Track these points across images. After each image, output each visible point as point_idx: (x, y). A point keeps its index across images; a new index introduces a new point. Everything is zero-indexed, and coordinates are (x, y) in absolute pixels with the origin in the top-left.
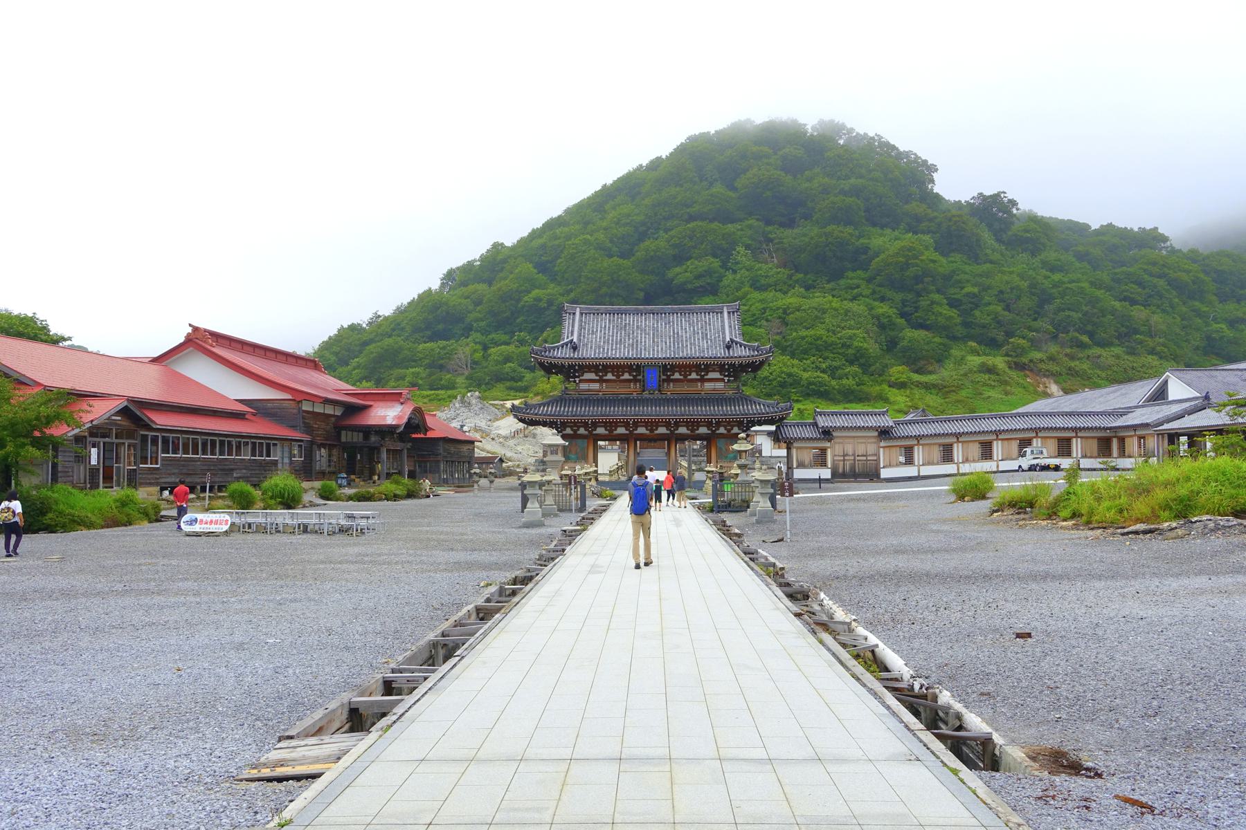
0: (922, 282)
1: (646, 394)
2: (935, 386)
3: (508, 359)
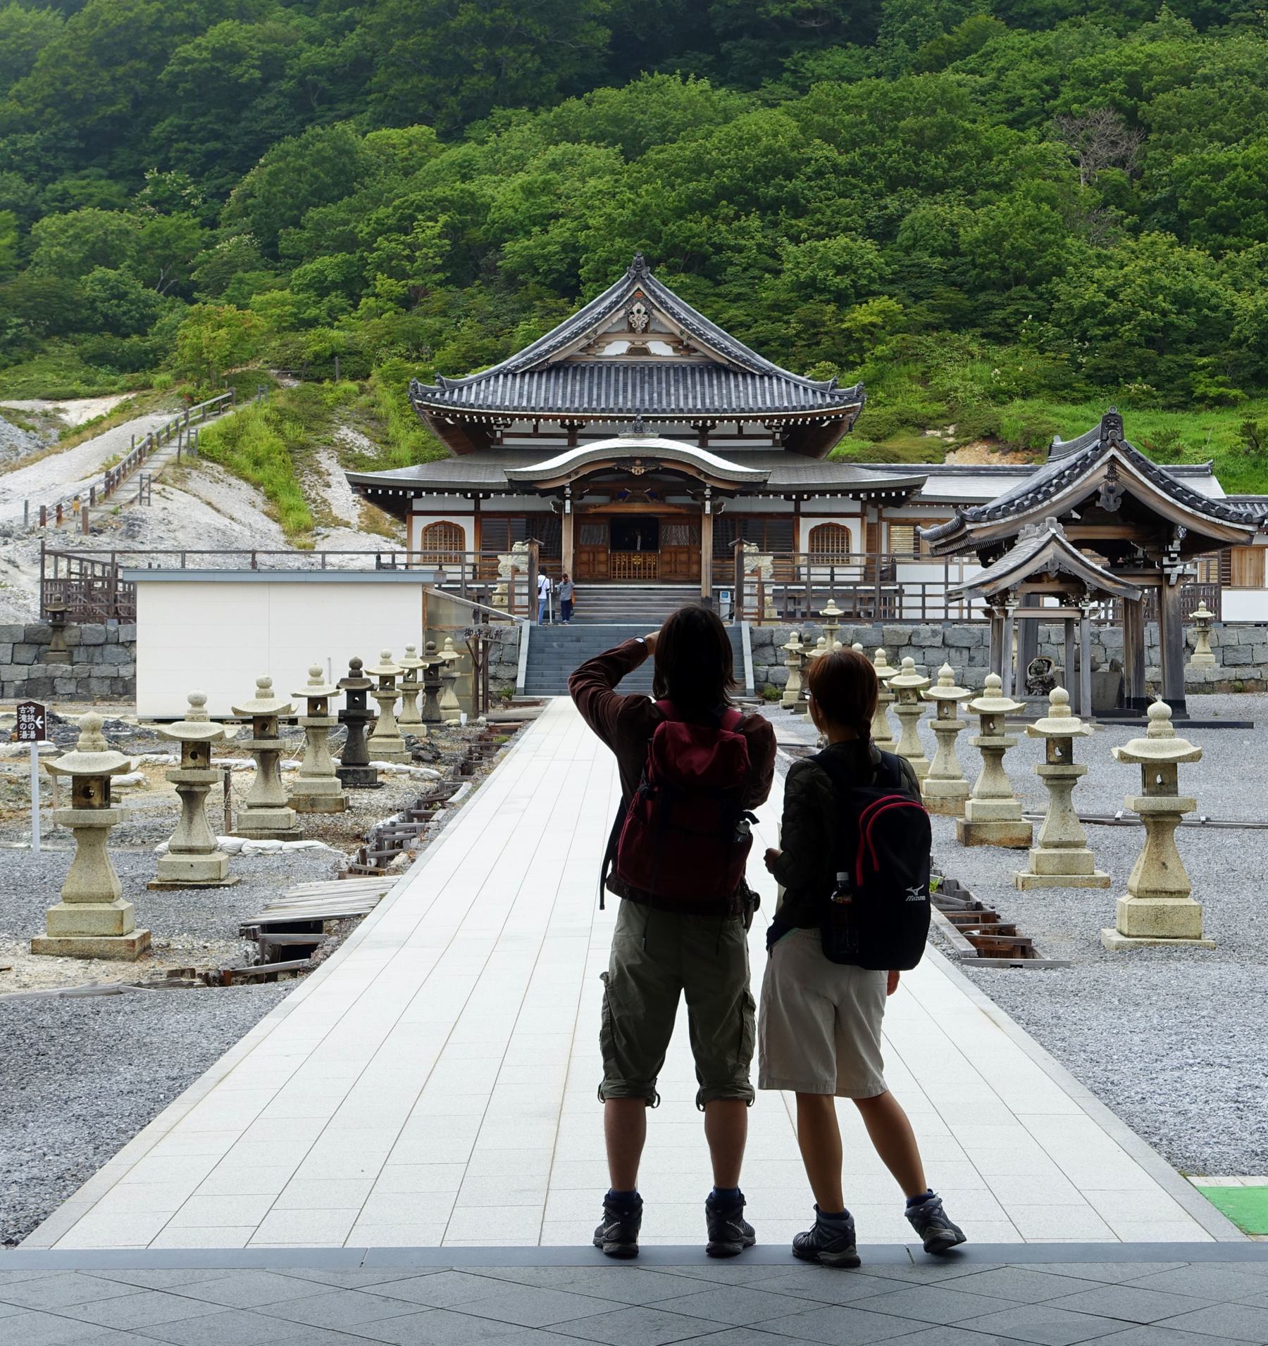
3: (103, 254)
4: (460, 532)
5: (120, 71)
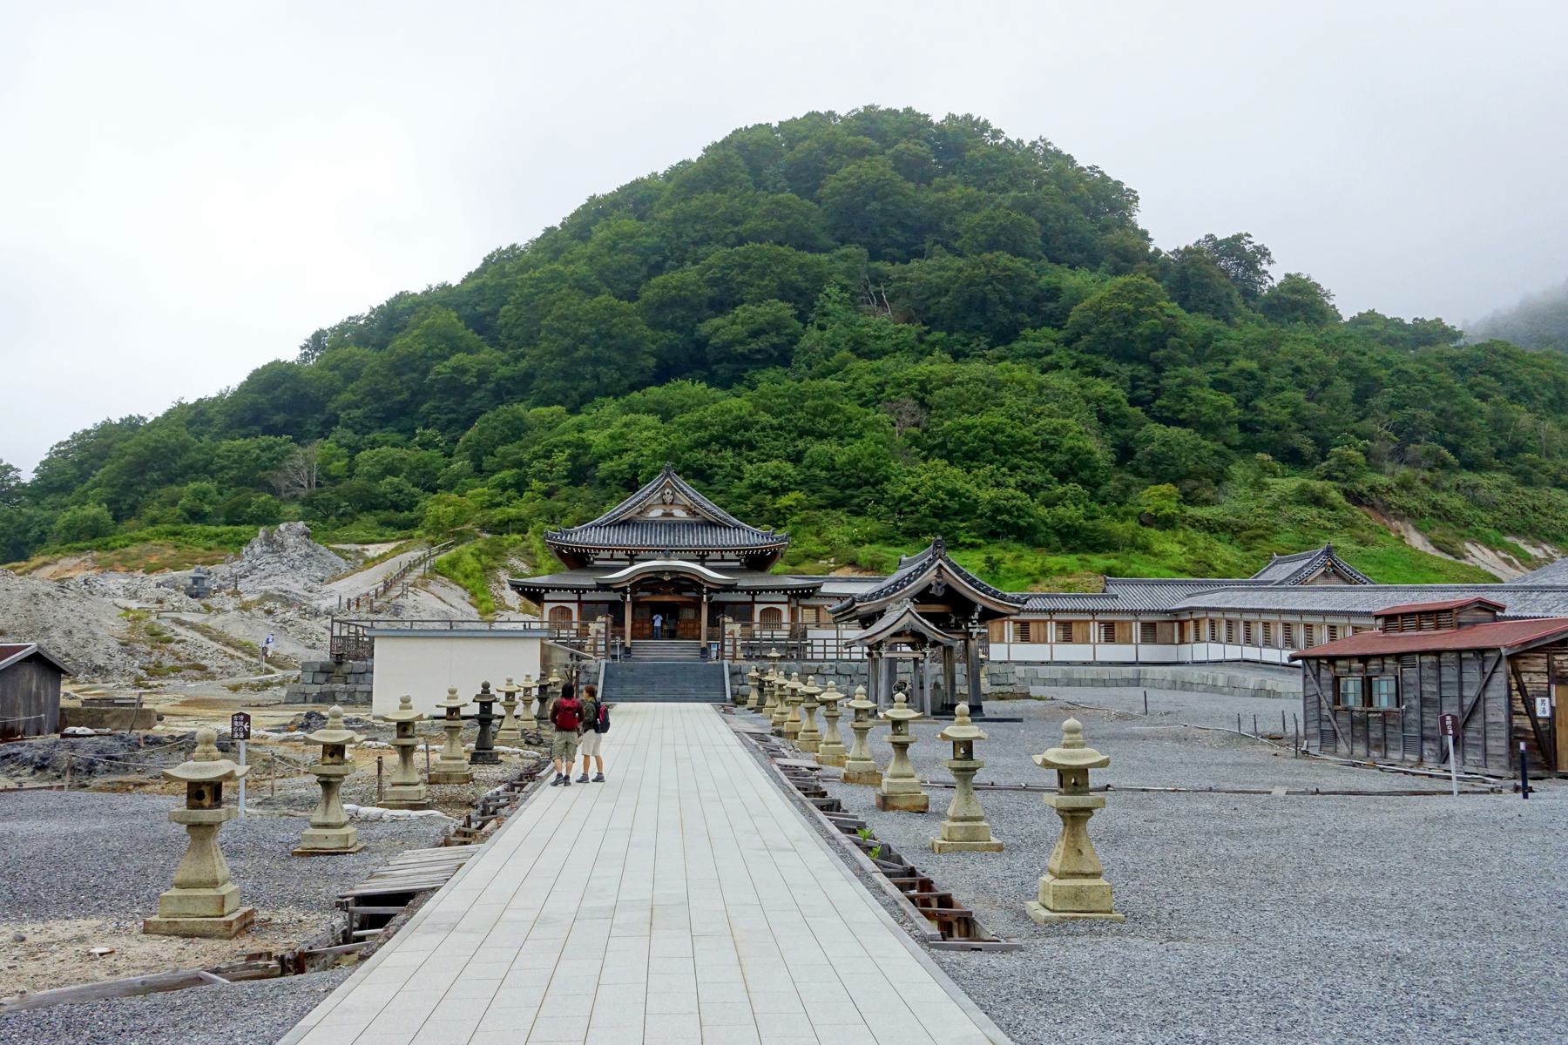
0: (1165, 347)
2: (1224, 527)
3: (392, 470)
4: (570, 611)
5: (404, 378)
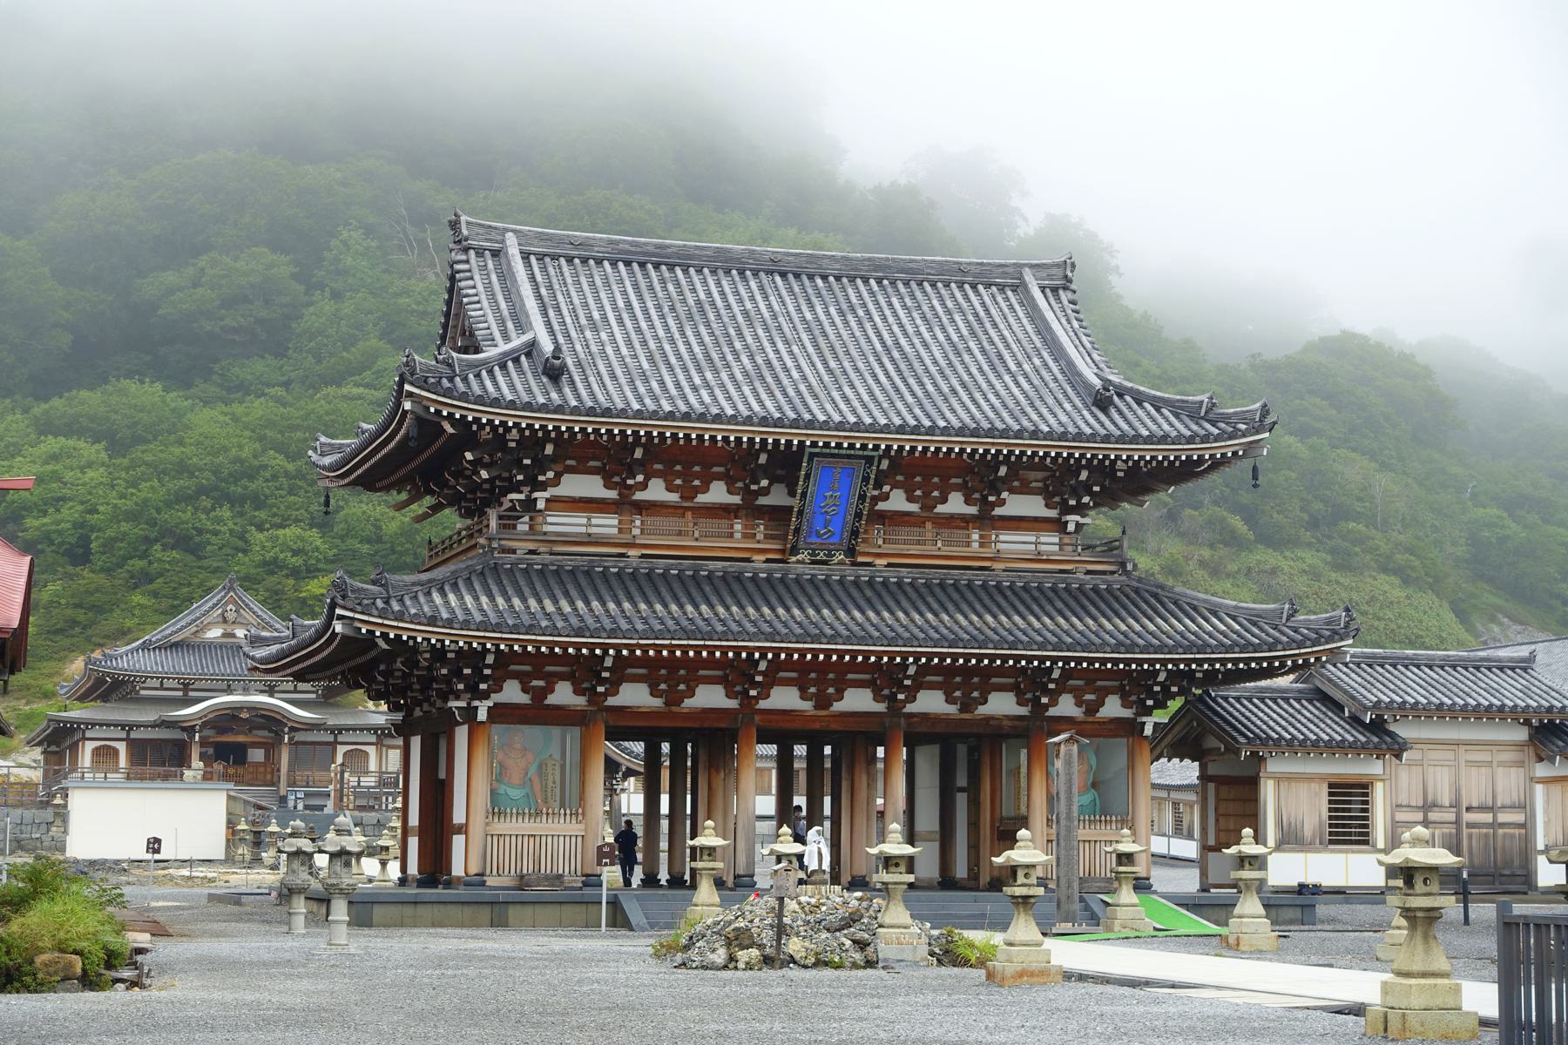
1: (800, 565)
4: (116, 752)
